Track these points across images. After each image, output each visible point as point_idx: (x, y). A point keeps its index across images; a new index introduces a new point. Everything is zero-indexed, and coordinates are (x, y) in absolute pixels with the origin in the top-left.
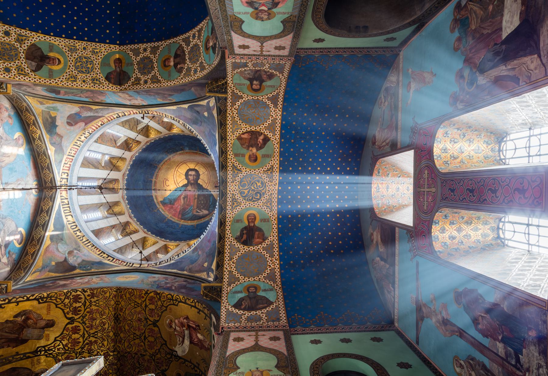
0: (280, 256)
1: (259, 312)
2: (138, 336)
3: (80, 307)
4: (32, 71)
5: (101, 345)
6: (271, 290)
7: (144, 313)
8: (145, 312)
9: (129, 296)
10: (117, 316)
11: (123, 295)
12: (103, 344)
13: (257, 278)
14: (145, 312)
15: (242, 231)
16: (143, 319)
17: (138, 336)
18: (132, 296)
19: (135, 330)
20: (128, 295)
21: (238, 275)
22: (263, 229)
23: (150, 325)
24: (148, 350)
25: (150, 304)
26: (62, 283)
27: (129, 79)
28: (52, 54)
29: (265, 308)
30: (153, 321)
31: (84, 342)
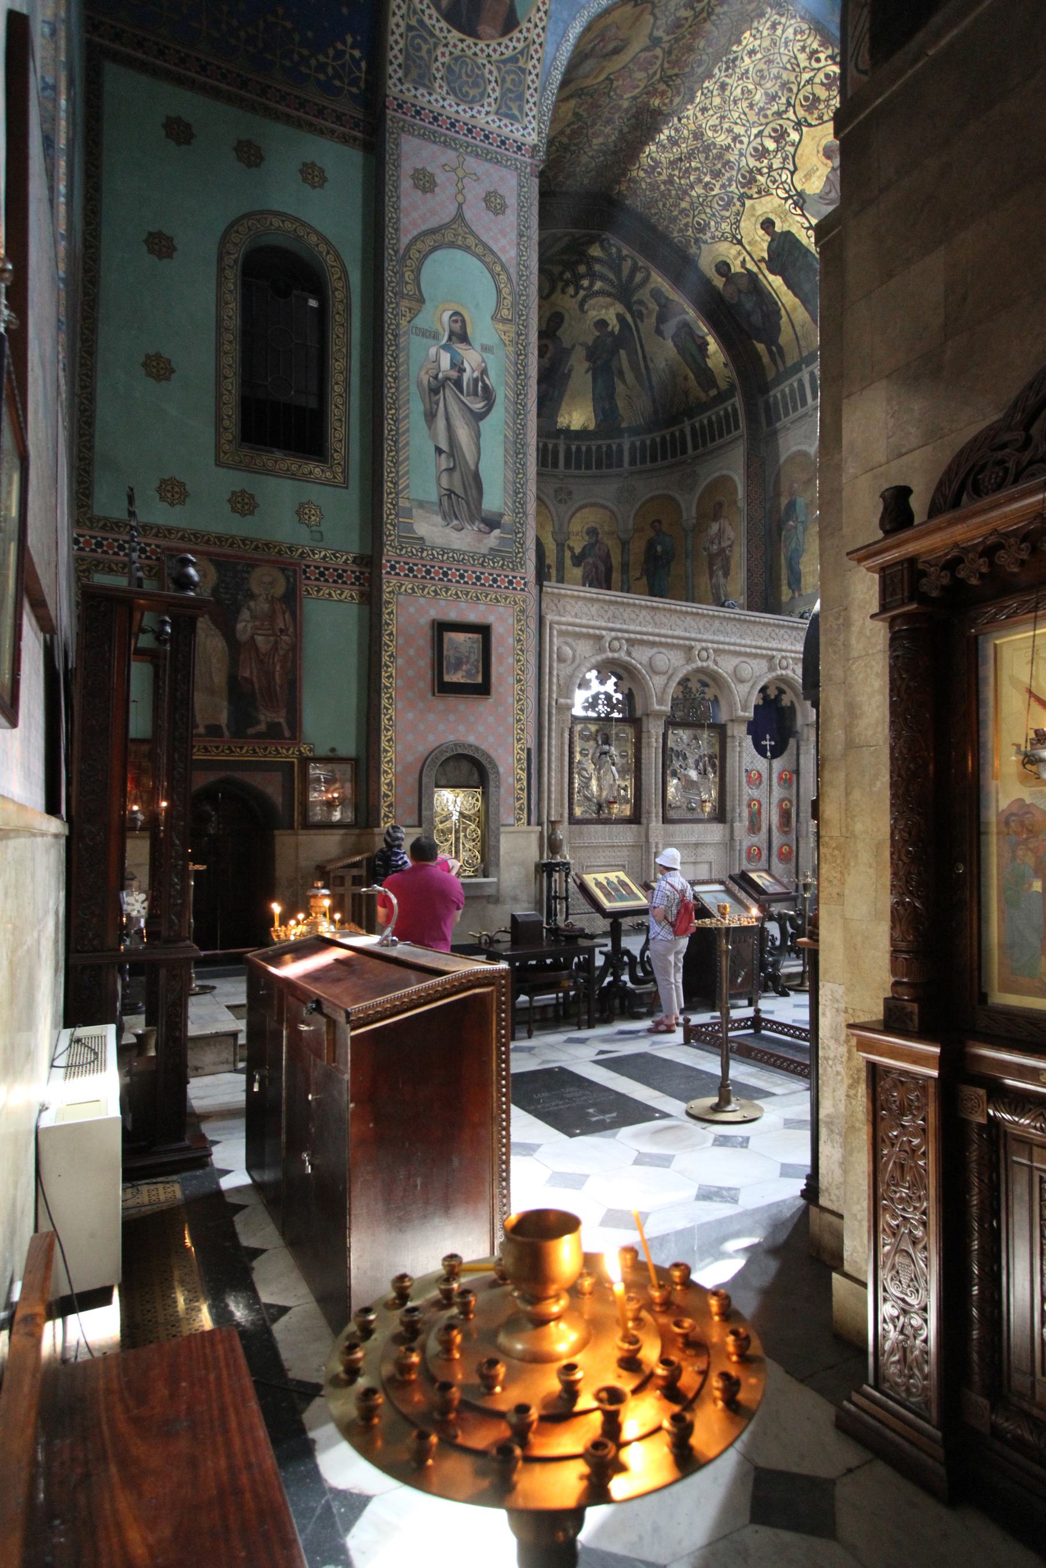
2: (748, 121)
3: (686, 19)
5: (667, 101)
7: (795, 90)
8: (799, 90)
9: (791, 37)
10: (736, 59)
11: (780, 23)
12: (671, 102)
14: (799, 90)
16: (784, 100)
17: (748, 121)
18: (799, 41)
19: (751, 106)
20: (791, 31)
23: (788, 119)
24: (748, 156)
25: (822, 84)
30: (799, 117)
31: (646, 87)
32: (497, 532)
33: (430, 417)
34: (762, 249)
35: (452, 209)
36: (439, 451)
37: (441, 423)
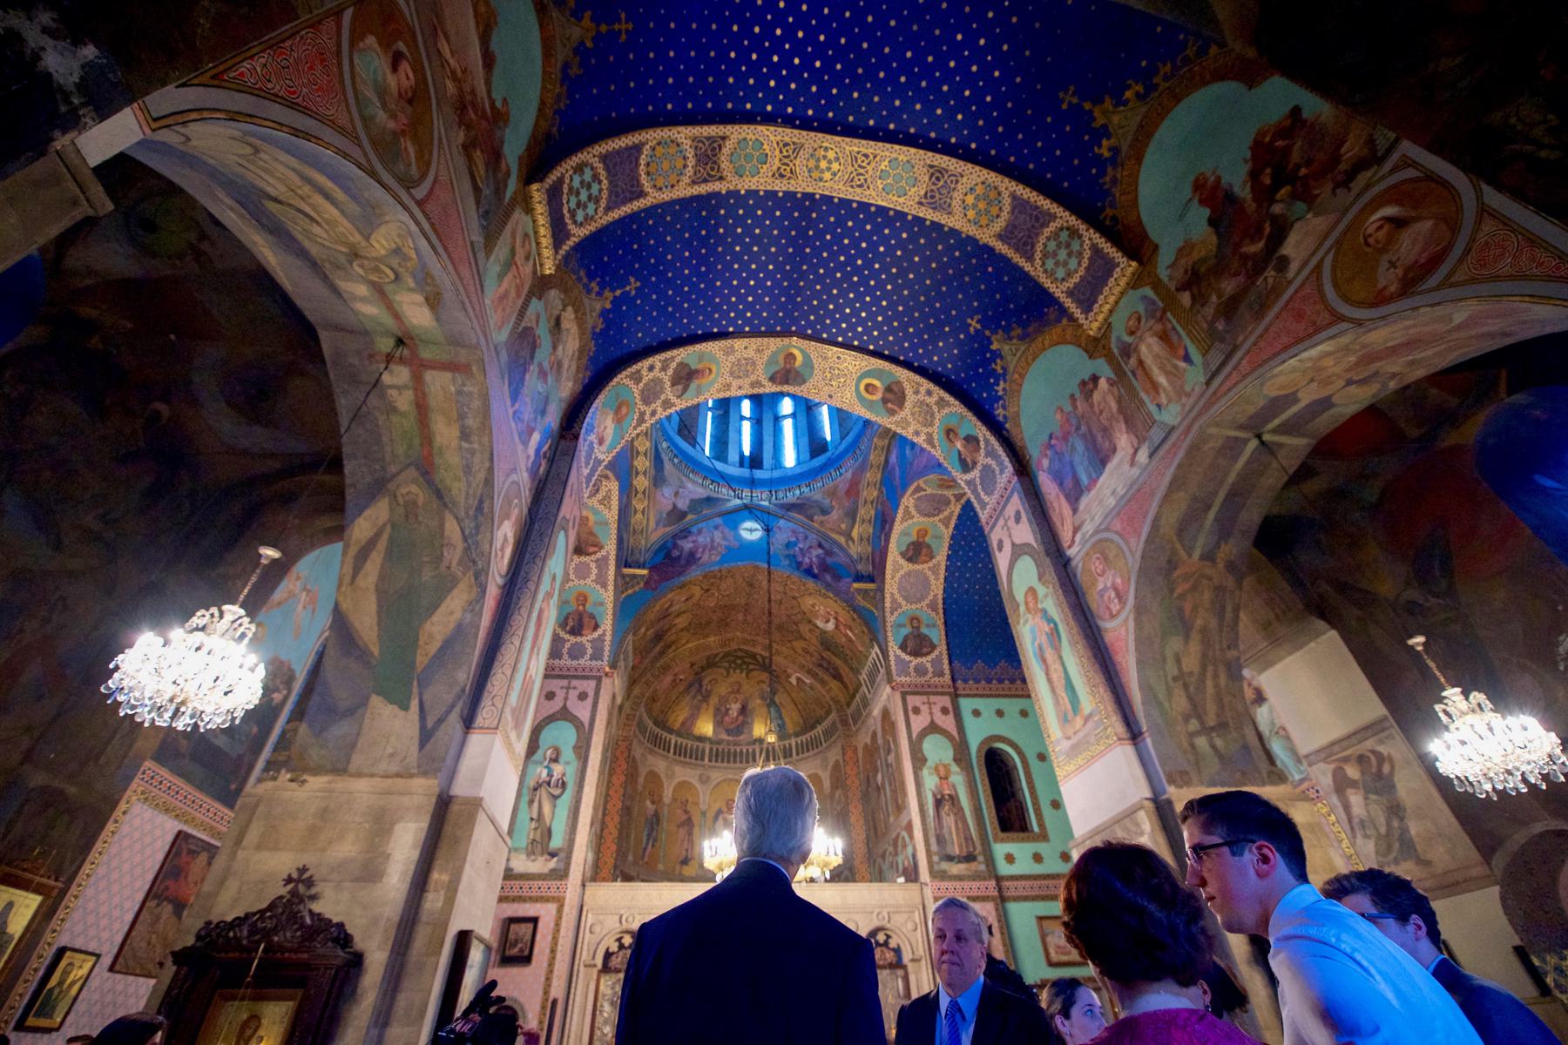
0: (946, 578)
1: (924, 660)
4: (679, 397)
6: (934, 625)
13: (919, 606)
15: (909, 545)
21: (900, 600)
22: (933, 546)
26: (687, 545)
27: (804, 382)
28: (700, 366)
29: (928, 653)
32: (555, 859)
33: (531, 802)
34: (814, 641)
35: (561, 704)
36: (532, 819)
37: (536, 805)
